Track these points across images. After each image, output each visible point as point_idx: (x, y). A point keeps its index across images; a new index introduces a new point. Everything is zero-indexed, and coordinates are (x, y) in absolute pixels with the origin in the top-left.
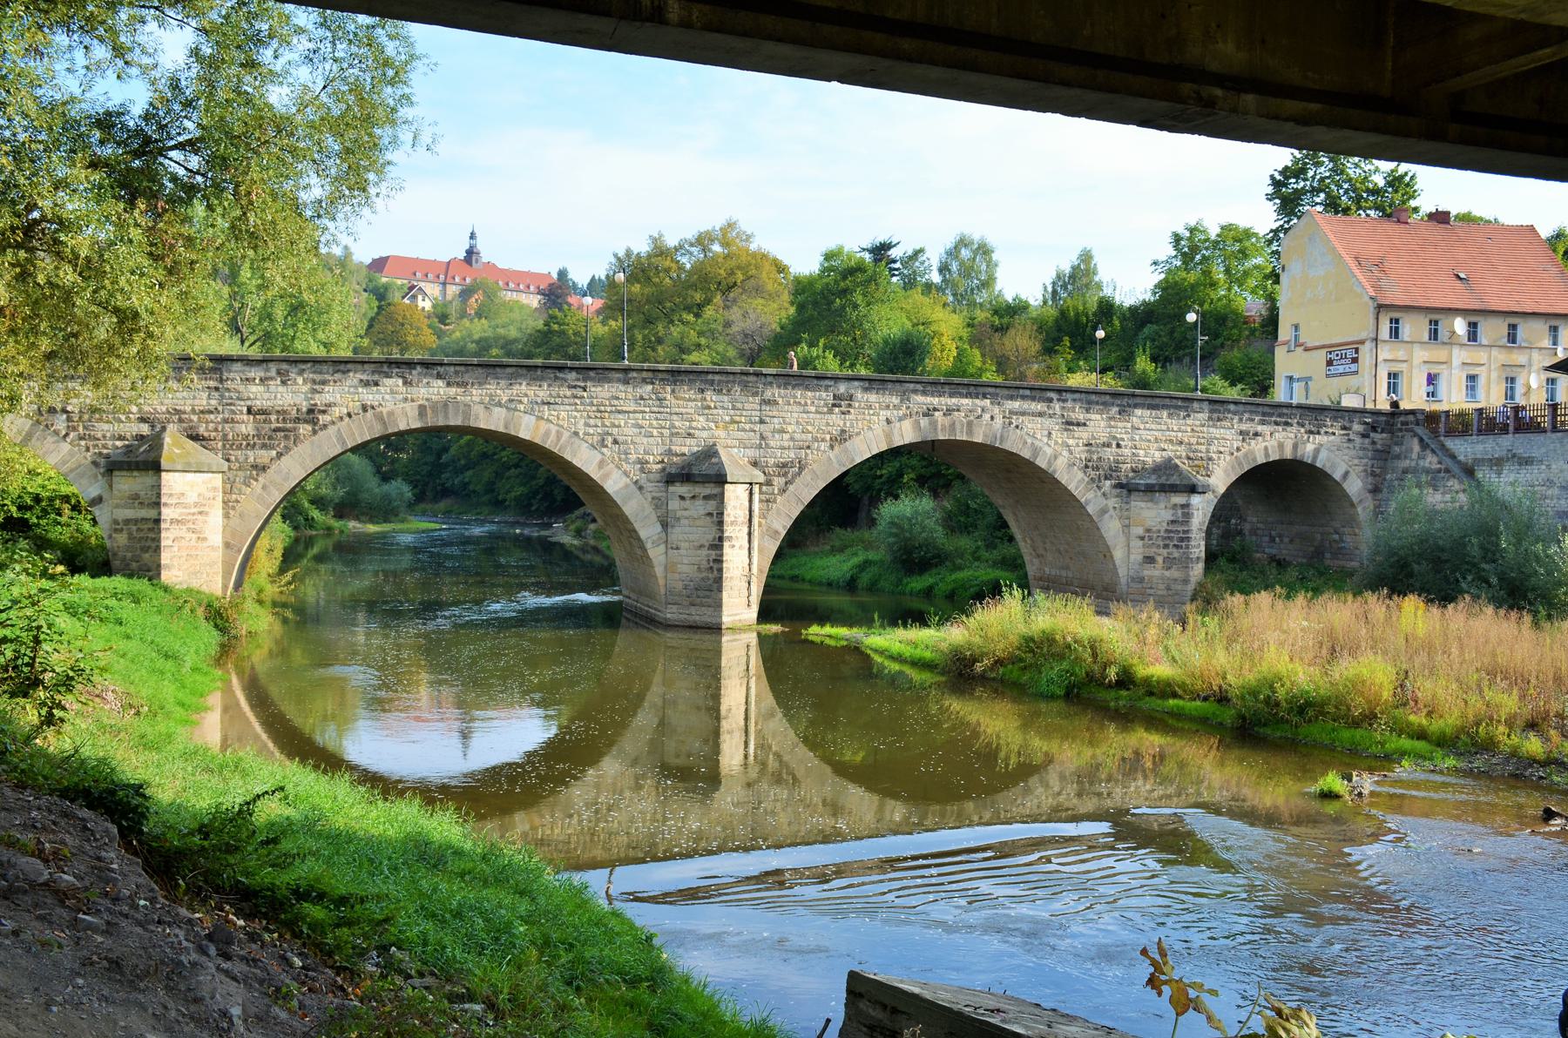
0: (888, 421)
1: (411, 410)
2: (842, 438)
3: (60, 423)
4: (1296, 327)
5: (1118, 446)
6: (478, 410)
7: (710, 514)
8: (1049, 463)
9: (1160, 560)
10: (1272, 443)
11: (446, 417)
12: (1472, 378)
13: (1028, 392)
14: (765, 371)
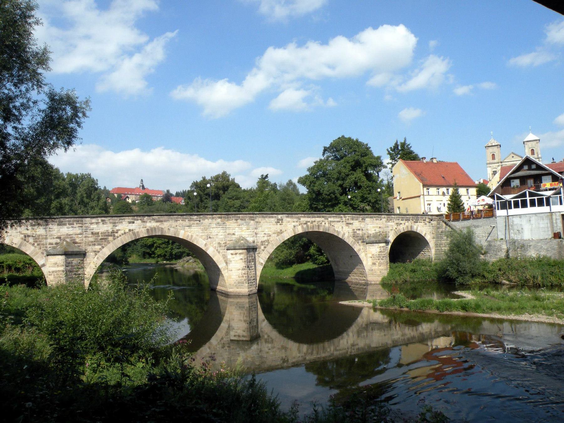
0: (294, 227)
1: (144, 230)
2: (281, 232)
3: (31, 240)
4: (399, 193)
8: (343, 236)
9: (377, 263)
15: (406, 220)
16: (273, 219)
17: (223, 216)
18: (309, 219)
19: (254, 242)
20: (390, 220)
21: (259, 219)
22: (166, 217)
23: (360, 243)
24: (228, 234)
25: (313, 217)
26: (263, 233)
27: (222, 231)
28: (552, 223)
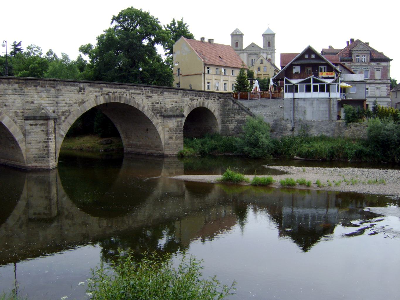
0: (96, 97)
5: (160, 103)
7: (43, 131)
9: (174, 137)
10: (197, 102)
12: (225, 84)
13: (136, 87)
15: (199, 96)
16: (74, 88)
17: (21, 81)
20: (186, 95)
23: (158, 117)
24: (27, 102)
25: (115, 88)
26: (64, 102)
27: (19, 98)
28: (330, 107)
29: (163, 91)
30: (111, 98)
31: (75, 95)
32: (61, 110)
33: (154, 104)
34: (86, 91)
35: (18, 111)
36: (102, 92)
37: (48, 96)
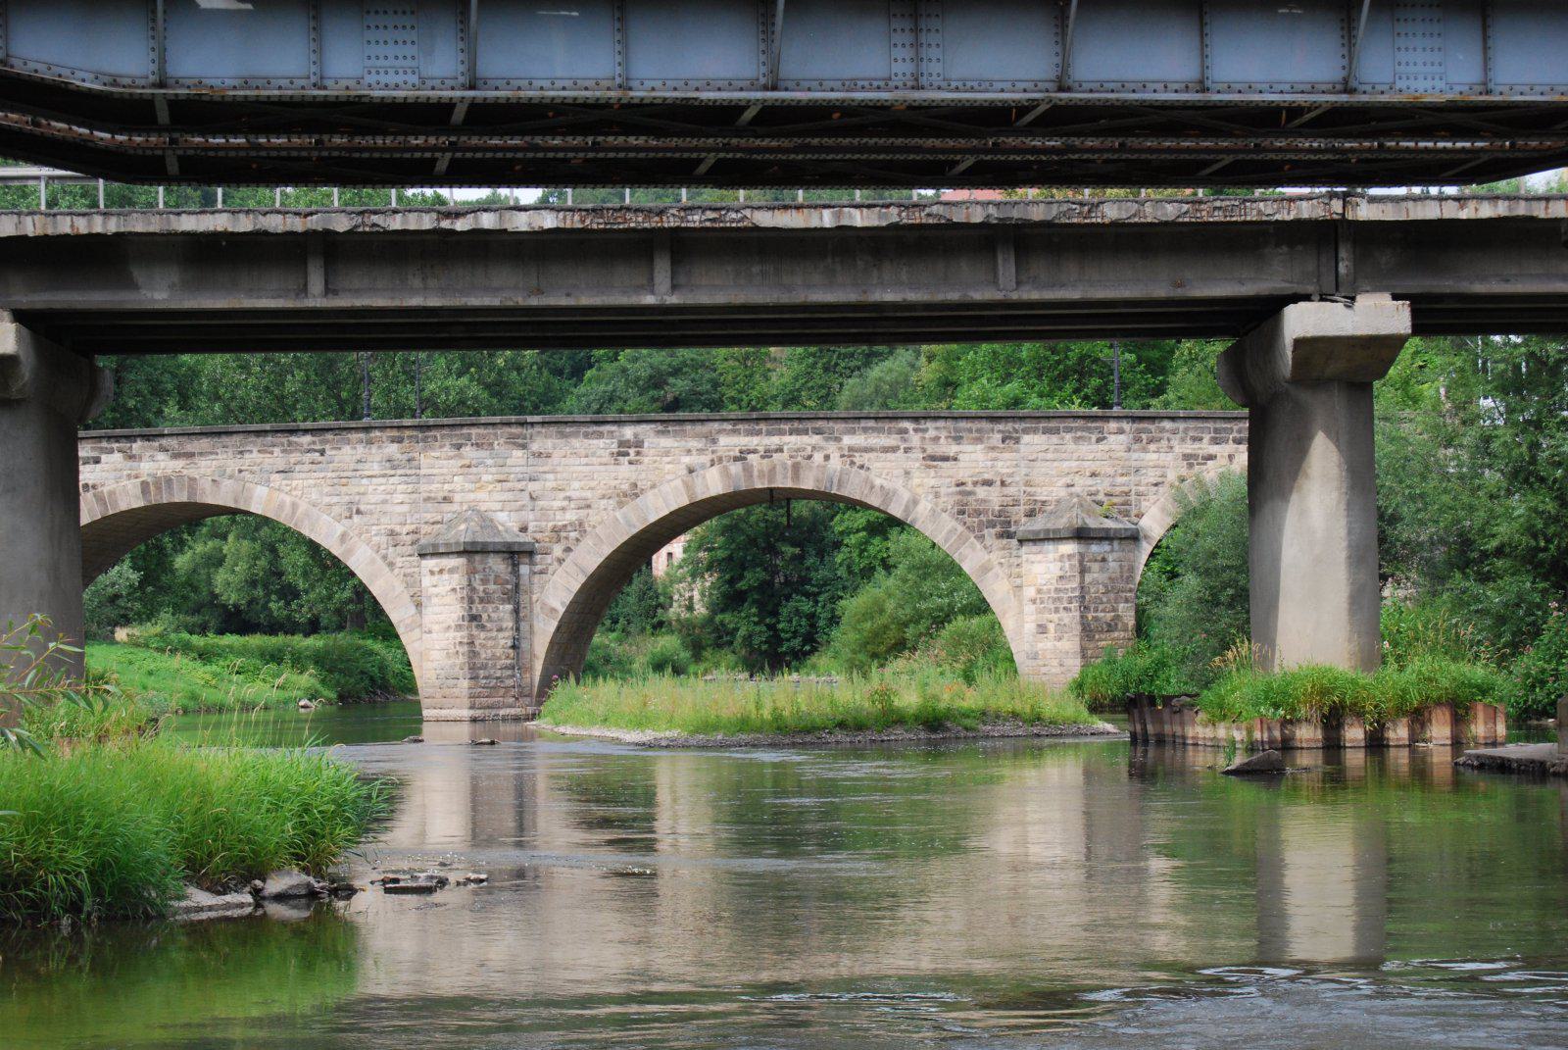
0: (691, 471)
2: (635, 492)
5: (1003, 483)
6: (205, 484)
8: (907, 510)
11: (171, 494)
14: (530, 419)
16: (601, 443)
17: (407, 433)
18: (753, 442)
19: (524, 529)
21: (543, 441)
22: (204, 443)
23: (989, 541)
24: (427, 499)
25: (769, 433)
26: (562, 495)
27: (401, 488)
29: (1017, 431)
30: (756, 473)
31: (602, 468)
32: (550, 524)
33: (969, 488)
34: (644, 450)
35: (398, 529)
36: (713, 452)
37: (502, 477)
